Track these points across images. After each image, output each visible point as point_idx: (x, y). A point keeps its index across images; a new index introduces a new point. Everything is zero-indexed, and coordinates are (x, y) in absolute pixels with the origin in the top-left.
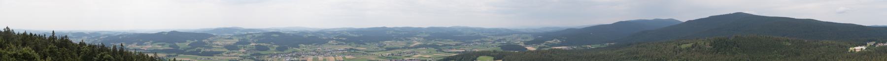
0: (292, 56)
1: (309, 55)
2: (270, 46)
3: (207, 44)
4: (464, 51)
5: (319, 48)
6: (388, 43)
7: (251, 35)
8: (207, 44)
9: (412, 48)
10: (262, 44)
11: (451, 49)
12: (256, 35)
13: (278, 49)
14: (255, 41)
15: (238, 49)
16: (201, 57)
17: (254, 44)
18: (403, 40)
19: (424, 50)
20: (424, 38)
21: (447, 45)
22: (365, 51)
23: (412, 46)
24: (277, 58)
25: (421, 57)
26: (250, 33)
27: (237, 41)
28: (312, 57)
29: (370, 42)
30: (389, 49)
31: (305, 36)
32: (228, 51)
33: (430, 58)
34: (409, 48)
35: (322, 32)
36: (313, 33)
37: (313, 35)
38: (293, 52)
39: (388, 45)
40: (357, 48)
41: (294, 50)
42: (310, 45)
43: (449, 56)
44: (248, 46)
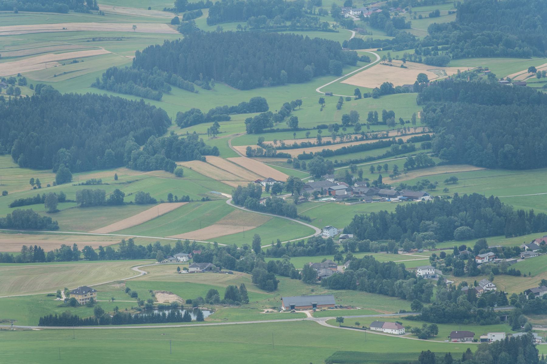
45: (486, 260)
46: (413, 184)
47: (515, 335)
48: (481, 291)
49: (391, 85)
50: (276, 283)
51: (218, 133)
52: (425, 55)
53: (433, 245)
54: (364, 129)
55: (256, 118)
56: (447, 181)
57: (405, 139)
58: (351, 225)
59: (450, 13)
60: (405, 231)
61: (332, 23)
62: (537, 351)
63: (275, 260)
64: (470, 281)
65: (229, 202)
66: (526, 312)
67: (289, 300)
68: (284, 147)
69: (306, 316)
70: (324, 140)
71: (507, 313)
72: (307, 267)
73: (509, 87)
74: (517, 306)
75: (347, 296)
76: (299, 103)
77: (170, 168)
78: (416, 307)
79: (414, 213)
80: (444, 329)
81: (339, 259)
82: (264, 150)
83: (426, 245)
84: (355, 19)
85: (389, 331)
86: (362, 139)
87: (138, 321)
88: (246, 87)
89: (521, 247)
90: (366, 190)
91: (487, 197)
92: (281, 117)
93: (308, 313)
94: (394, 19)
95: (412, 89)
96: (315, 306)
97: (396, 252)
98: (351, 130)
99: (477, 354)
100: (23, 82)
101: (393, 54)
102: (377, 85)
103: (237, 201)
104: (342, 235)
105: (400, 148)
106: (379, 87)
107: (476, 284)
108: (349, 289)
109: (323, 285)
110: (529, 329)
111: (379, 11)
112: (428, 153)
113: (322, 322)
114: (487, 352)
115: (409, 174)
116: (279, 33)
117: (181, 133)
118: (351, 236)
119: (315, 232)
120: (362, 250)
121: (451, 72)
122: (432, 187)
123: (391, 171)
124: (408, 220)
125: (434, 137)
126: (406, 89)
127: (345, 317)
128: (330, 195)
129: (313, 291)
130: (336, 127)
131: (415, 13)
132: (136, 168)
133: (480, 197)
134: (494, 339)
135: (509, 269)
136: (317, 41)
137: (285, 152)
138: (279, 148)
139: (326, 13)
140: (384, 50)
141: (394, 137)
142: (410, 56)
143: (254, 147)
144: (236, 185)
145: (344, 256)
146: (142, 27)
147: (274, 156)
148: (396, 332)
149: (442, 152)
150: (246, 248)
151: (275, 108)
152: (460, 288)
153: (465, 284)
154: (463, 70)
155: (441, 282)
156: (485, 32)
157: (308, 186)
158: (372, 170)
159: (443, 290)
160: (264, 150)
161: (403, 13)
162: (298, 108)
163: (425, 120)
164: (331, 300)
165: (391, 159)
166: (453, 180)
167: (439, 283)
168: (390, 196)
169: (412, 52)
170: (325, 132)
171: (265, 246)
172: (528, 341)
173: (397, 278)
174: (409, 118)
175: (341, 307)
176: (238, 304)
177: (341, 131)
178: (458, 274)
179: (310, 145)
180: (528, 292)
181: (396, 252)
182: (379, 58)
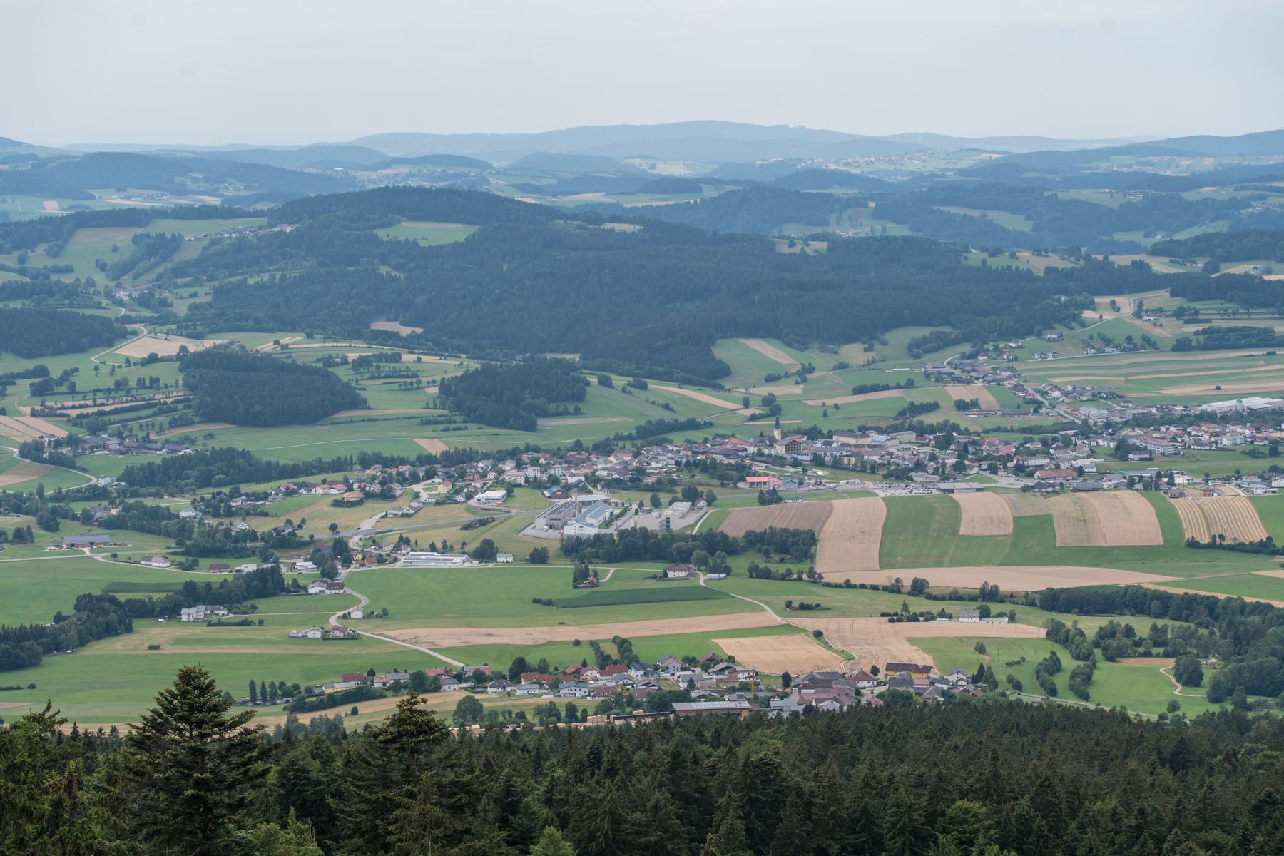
0: (634, 481)
1: (837, 465)
2: (362, 363)
7: (124, 237)
10: (263, 344)
12: (195, 235)
14: (181, 308)
17: (168, 346)
24: (459, 513)
26: (113, 200)
28: (882, 490)
37: (898, 230)
38: (653, 434)
41: (659, 415)
42: (854, 353)
45: (239, 503)
46: (175, 440)
47: (265, 566)
48: (235, 530)
49: (156, 355)
50: (58, 525)
51: (5, 395)
52: (185, 330)
53: (194, 491)
54: (134, 392)
55: (39, 383)
56: (205, 436)
57: (169, 401)
58: (123, 474)
59: (206, 294)
60: (170, 479)
61: (105, 302)
62: (283, 580)
63: (57, 504)
64: (226, 521)
65: (15, 455)
66: (274, 547)
68: (63, 408)
69: (84, 552)
70: (99, 402)
71: (257, 548)
72: (85, 511)
73: (258, 357)
74: (266, 542)
75: (119, 536)
76: (77, 370)
78: (180, 544)
79: (178, 464)
80: (204, 562)
81: (112, 503)
82: (46, 411)
83: (187, 492)
84: (125, 298)
85: (158, 564)
86: (131, 401)
88: (29, 356)
89: (269, 491)
90: (136, 445)
91: (240, 450)
93: (87, 550)
94: (158, 299)
95: (174, 358)
96: (92, 544)
97: (162, 497)
98: (122, 393)
99: (232, 583)
101: (158, 328)
102: (144, 354)
103: (23, 454)
104: (115, 483)
105: (165, 408)
106: (146, 356)
107: (231, 524)
108: (122, 529)
109: (99, 526)
110: (276, 561)
111: (146, 291)
112: (189, 413)
113: (99, 557)
114: (241, 581)
115: (173, 431)
116: (59, 310)
118: (123, 484)
119: (91, 480)
120: (132, 496)
121: (208, 344)
122: (193, 442)
123: (157, 428)
124: (172, 470)
125: (194, 399)
126: (169, 359)
127: (119, 553)
128: (105, 449)
129: (90, 531)
130: (109, 391)
131: (177, 294)
133: (234, 450)
134: (247, 570)
135: (258, 510)
136: (92, 317)
137: (65, 412)
138: (60, 409)
139: (100, 293)
140: (150, 325)
141: (159, 400)
142: (173, 330)
143: (38, 408)
144: (22, 441)
145: (117, 501)
147: (55, 415)
148: (164, 565)
149: (201, 411)
150: (31, 494)
151: (55, 374)
152: (217, 527)
153: (222, 524)
154: (218, 342)
155: (201, 522)
156: (236, 311)
157: (85, 441)
158: (141, 427)
159: (203, 529)
160: (46, 411)
161: (166, 294)
162: (75, 374)
163: (186, 385)
164: (106, 538)
165: (157, 418)
166: (211, 436)
167: (199, 523)
168: (156, 450)
169: (174, 327)
170: (100, 395)
171: (48, 493)
172: (275, 571)
173: (164, 520)
174: (171, 382)
175: (115, 544)
176: (24, 543)
177: (113, 394)
178: (216, 515)
179: (87, 406)
180: (275, 529)
181: (162, 497)
182: (146, 332)
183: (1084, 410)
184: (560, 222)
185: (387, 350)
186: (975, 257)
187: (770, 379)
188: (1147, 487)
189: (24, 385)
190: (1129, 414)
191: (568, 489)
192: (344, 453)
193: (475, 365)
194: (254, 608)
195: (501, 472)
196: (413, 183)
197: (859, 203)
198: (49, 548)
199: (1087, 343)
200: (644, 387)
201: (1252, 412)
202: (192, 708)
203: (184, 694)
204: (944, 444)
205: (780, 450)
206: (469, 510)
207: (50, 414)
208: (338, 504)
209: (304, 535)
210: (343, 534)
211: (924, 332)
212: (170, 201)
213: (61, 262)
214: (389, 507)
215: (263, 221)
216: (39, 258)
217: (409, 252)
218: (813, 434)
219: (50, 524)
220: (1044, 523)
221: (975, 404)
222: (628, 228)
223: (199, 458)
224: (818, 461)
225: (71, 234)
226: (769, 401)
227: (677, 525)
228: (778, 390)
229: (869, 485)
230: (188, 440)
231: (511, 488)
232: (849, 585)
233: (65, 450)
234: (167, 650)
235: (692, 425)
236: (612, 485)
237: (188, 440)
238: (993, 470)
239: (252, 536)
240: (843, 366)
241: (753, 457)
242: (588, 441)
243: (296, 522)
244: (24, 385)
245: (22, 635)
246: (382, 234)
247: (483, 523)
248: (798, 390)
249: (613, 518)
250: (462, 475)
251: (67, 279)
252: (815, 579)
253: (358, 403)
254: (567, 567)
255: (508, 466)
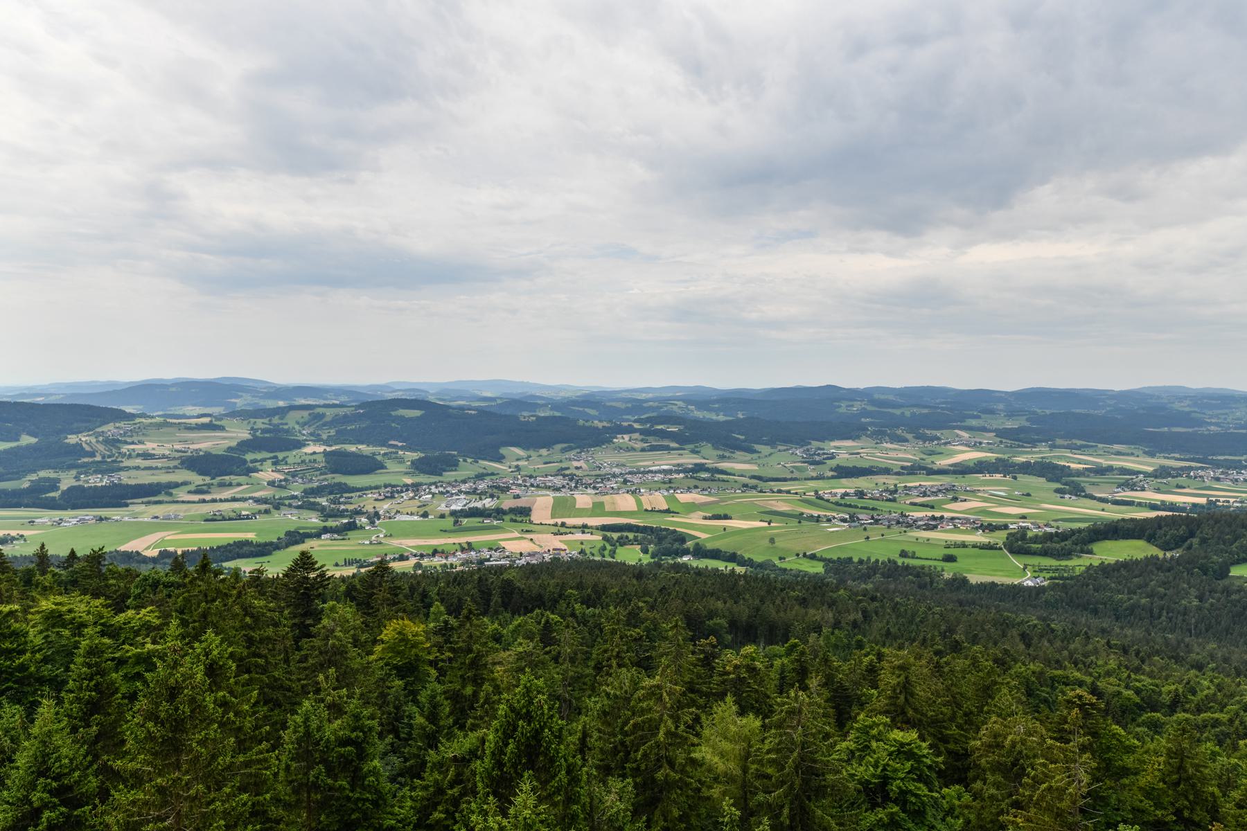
0: (474, 492)
1: (538, 486)
2: (385, 454)
3: (92, 454)
4: (1203, 501)
5: (579, 463)
6: (843, 451)
7: (305, 414)
8: (92, 454)
9: (941, 472)
10: (352, 448)
11: (1132, 487)
12: (330, 413)
13: (419, 467)
14: (324, 437)
15: (248, 471)
16: (57, 514)
18: (907, 441)
19: (998, 483)
20: (1002, 434)
21: (1110, 469)
22: (753, 477)
23: (943, 462)
25: (984, 512)
26: (303, 402)
27: (245, 435)
28: (552, 494)
29: (772, 443)
30: (844, 472)
31: (525, 415)
32: (197, 479)
33: (1024, 517)
34: (931, 472)
35: (591, 401)
36: (556, 406)
37: (557, 414)
38: (480, 477)
39: (843, 458)
40: (724, 465)
41: (481, 471)
42: (544, 452)
43: (1120, 516)
44: (293, 456)
67: (283, 513)
75: (301, 511)
77: (247, 475)
80: (330, 519)
85: (314, 520)
87: (236, 519)
88: (272, 452)
92: (282, 461)
100: (201, 450)
102: (312, 452)
113: (294, 518)
117: (251, 465)
121: (333, 448)
122: (327, 480)
126: (320, 453)
132: (236, 475)
146: (239, 435)
171: (277, 497)
172: (354, 522)
178: (335, 504)
183: (614, 469)
184: (451, 410)
185: (394, 450)
186: (581, 422)
187: (518, 460)
188: (633, 493)
189: (269, 462)
190: (627, 471)
191: (452, 494)
192: (379, 483)
193: (423, 455)
194: (347, 534)
195: (430, 489)
196: (403, 397)
197: (545, 405)
198: (276, 516)
199: (615, 449)
200: (477, 462)
201: (664, 470)
202: (304, 564)
203: (302, 559)
204: (571, 480)
205: (520, 482)
206: (420, 501)
207: (279, 471)
208: (376, 500)
209: (364, 510)
210: (378, 510)
211: (566, 445)
212: (322, 402)
213: (284, 421)
214: (394, 501)
215: (353, 409)
216: (276, 420)
217: (401, 419)
218: (531, 477)
219: (277, 507)
220: (602, 503)
221: (581, 467)
222: (473, 412)
223: (329, 485)
224: (532, 485)
225: (288, 412)
226: (517, 467)
227: (487, 506)
228: (520, 463)
229: (548, 493)
230: (326, 479)
231: (434, 494)
232: (541, 524)
233: (283, 483)
234: (316, 549)
235: (493, 474)
236: (466, 493)
237: (326, 479)
238: (586, 488)
239: (347, 510)
240: (541, 456)
241: (512, 484)
242: (459, 479)
243: (362, 506)
244: (269, 462)
245: (266, 544)
246: (393, 413)
247: (424, 505)
248: (526, 463)
249: (467, 504)
250: (418, 490)
251: (286, 427)
252: (531, 522)
253: (386, 468)
254: (452, 519)
255: (433, 487)
